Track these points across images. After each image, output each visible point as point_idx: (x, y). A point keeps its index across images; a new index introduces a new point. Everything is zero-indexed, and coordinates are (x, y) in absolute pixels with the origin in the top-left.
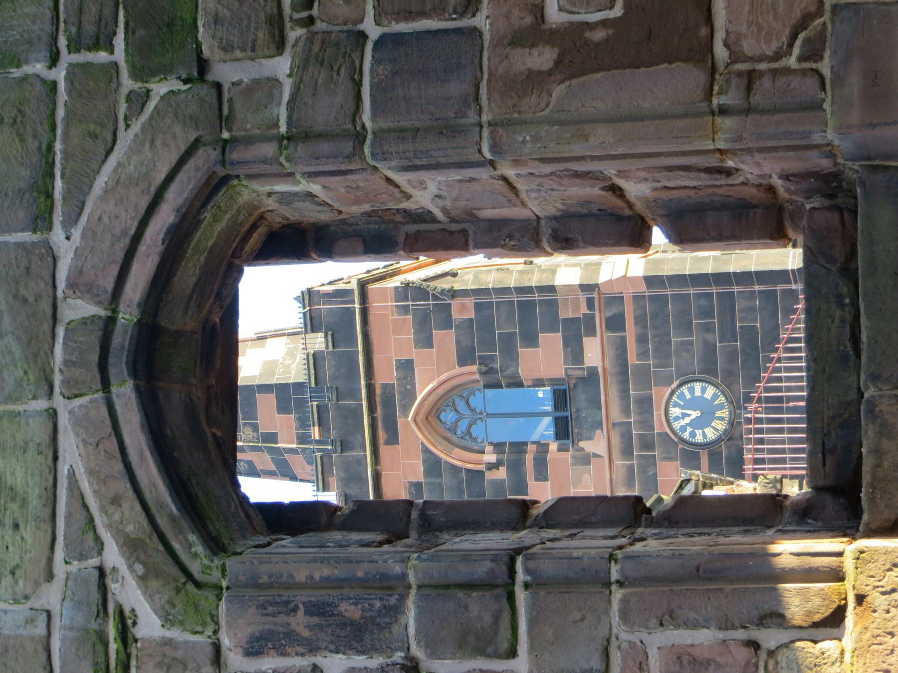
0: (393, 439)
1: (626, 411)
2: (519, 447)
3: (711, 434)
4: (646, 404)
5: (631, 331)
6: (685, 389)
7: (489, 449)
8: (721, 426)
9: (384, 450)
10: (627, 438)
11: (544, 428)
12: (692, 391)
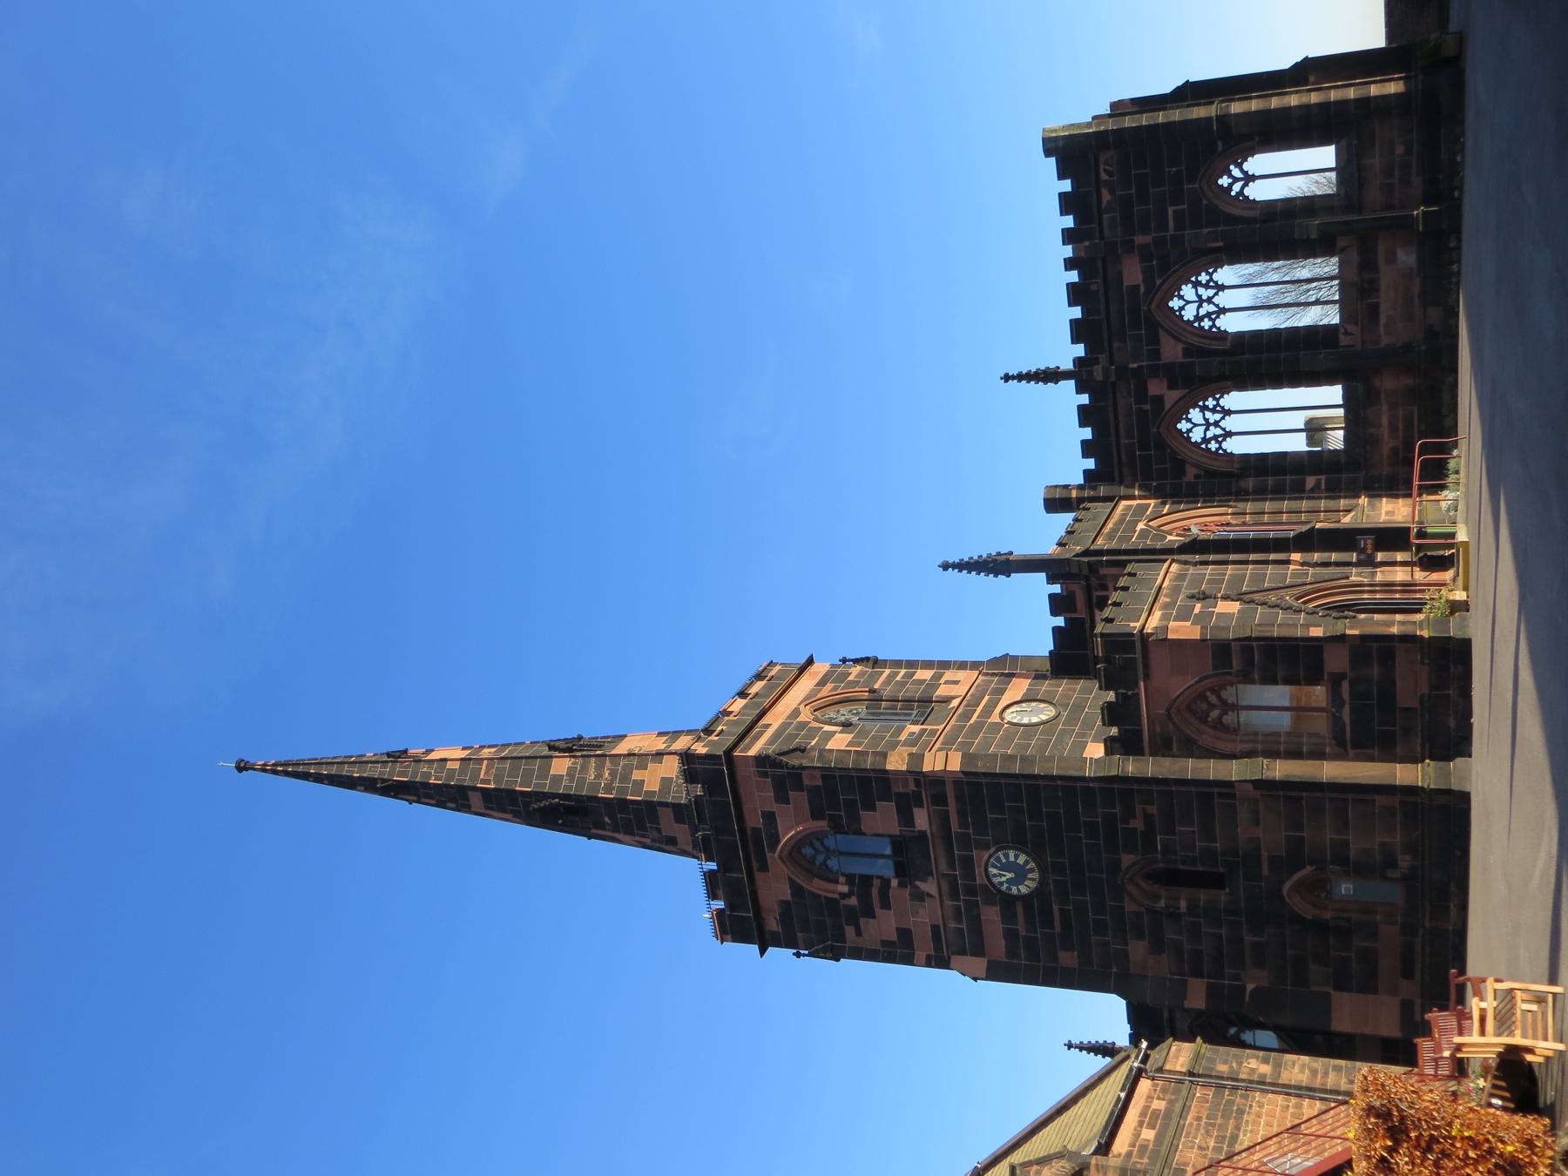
0: (764, 867)
1: (952, 865)
2: (866, 880)
3: (1024, 890)
4: (968, 863)
5: (952, 808)
6: (1000, 854)
7: (842, 879)
8: (1033, 885)
9: (759, 876)
10: (953, 881)
11: (885, 868)
12: (1007, 856)
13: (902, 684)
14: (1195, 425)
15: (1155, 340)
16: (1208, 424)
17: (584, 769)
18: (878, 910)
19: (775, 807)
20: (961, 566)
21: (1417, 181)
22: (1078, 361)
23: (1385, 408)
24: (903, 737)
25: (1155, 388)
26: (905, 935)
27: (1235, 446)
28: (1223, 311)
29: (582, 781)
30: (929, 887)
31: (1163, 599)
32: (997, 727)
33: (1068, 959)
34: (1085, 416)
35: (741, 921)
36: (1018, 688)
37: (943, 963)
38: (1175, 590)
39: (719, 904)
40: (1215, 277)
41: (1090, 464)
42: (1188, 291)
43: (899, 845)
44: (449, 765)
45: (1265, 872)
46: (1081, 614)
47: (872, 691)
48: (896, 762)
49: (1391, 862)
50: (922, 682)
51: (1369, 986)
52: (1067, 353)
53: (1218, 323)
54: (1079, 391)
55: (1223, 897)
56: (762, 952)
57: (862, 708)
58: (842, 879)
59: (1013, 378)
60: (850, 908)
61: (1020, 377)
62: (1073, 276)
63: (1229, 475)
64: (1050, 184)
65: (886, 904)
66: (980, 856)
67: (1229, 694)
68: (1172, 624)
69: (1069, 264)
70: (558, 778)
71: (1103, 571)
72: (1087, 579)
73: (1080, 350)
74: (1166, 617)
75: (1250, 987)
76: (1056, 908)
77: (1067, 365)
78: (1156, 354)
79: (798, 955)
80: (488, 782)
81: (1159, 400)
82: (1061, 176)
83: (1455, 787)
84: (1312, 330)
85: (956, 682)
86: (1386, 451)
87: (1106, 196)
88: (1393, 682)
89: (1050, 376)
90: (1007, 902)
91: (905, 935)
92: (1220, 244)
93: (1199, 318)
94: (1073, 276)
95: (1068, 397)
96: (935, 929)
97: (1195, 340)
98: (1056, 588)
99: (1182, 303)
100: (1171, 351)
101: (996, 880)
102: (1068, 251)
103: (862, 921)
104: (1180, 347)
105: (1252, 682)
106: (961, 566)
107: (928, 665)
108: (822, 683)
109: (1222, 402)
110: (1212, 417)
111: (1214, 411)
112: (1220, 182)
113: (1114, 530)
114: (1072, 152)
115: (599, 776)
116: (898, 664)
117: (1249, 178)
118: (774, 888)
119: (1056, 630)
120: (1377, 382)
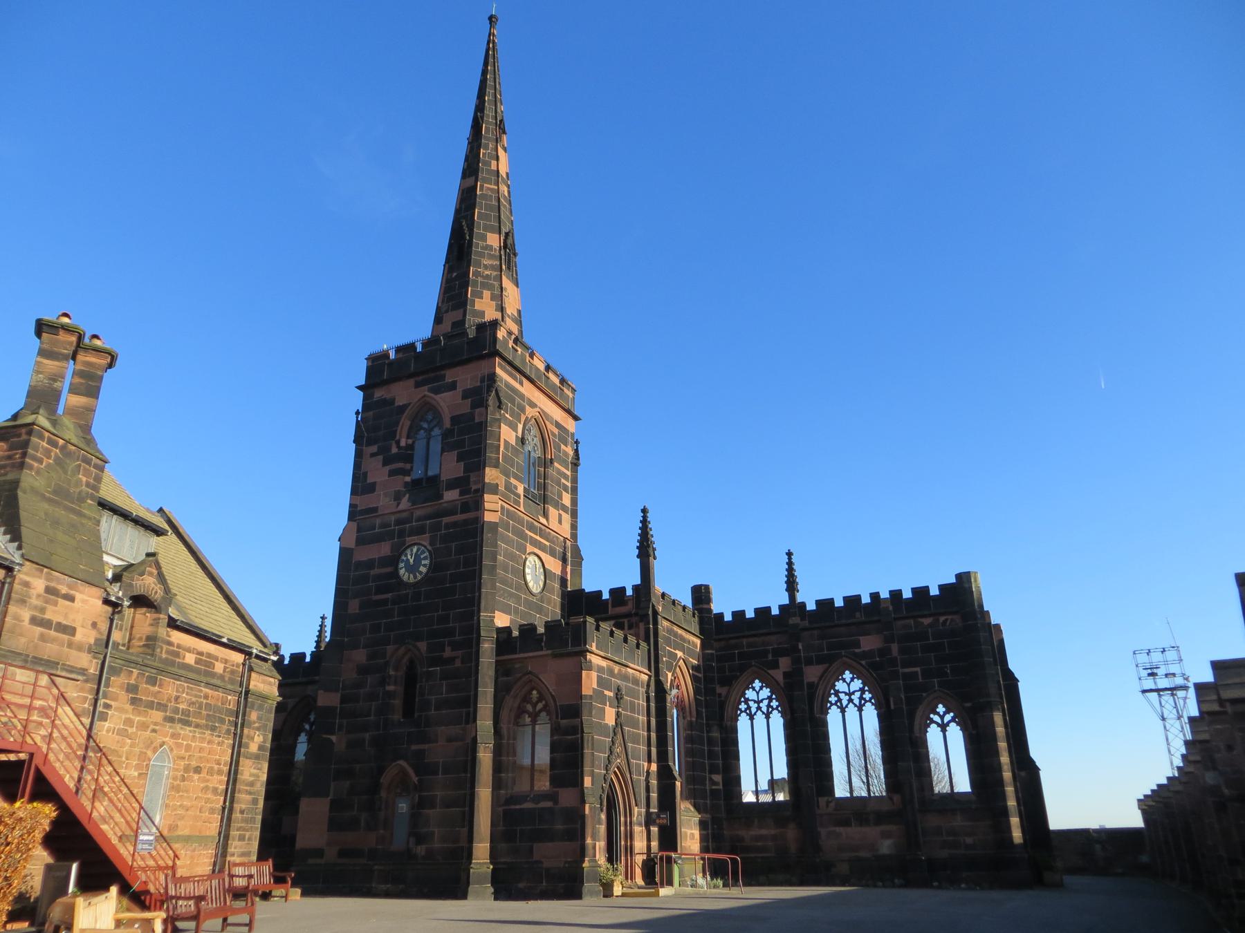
1: (419, 519)
2: (409, 459)
3: (402, 572)
4: (420, 531)
5: (460, 517)
6: (427, 554)
7: (410, 441)
8: (405, 578)
9: (411, 382)
10: (408, 520)
11: (418, 473)
12: (425, 558)
13: (559, 483)
14: (758, 692)
15: (820, 661)
16: (758, 702)
17: (491, 257)
18: (388, 468)
19: (460, 389)
20: (644, 522)
21: (944, 854)
22: (803, 605)
23: (773, 832)
24: (513, 481)
25: (785, 663)
26: (371, 488)
27: (743, 722)
28: (843, 710)
29: (482, 255)
30: (405, 503)
31: (616, 668)
32: (524, 551)
33: (354, 606)
34: (763, 612)
35: (381, 372)
36: (555, 566)
37: (352, 516)
38: (625, 678)
39: (392, 355)
40: (868, 704)
41: (728, 617)
42: (857, 684)
43: (434, 480)
44: (494, 163)
45: (414, 747)
46: (611, 611)
48: (491, 475)
49: (420, 839)
50: (561, 497)
51: (335, 825)
52: (808, 597)
53: (834, 707)
54: (781, 607)
55: (397, 717)
56: (359, 388)
57: (539, 453)
58: (410, 441)
59: (790, 559)
60: (390, 450)
61: (790, 564)
62: (866, 599)
63: (722, 718)
64: (935, 579)
65: (392, 473)
66: (425, 539)
68: (594, 675)
69: (875, 596)
70: (484, 238)
71: (642, 625)
72: (636, 614)
73: (811, 606)
74: (600, 669)
75: (334, 738)
76: (389, 595)
77: (800, 598)
78: (809, 662)
79: (357, 413)
80: (482, 189)
81: (775, 665)
82: (941, 587)
83: (471, 888)
84: (829, 776)
85: (560, 522)
86: (742, 833)
87: (927, 621)
88: (552, 840)
89: (791, 585)
90: (394, 560)
91: (371, 488)
92: (892, 707)
93: (837, 693)
94: (866, 599)
95: (776, 599)
96: (375, 510)
97: (820, 692)
98: (629, 592)
99: (848, 680)
100: (812, 673)
101: (408, 552)
102: (885, 595)
103: (381, 457)
104: (815, 680)
106: (644, 522)
107: (574, 502)
108: (558, 425)
109: (775, 712)
110: (764, 705)
111: (769, 706)
112: (940, 706)
113: (676, 635)
114: (960, 595)
115: (486, 267)
116: (575, 480)
117: (943, 727)
118: (403, 393)
119: (599, 593)
120: (792, 826)
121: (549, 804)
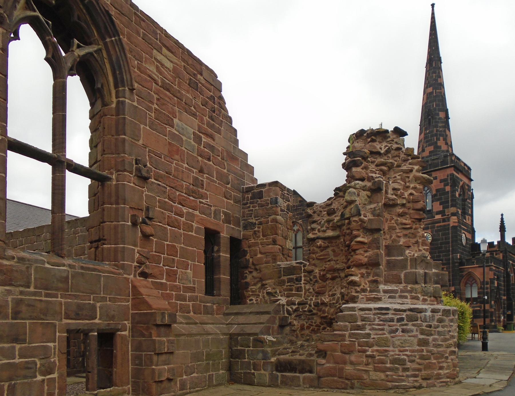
5: (442, 224)
32: (461, 232)
36: (469, 236)
47: (467, 199)
67: (474, 285)
74: (494, 270)
98: (496, 243)
105: (478, 289)
113: (510, 256)
121: (479, 308)
